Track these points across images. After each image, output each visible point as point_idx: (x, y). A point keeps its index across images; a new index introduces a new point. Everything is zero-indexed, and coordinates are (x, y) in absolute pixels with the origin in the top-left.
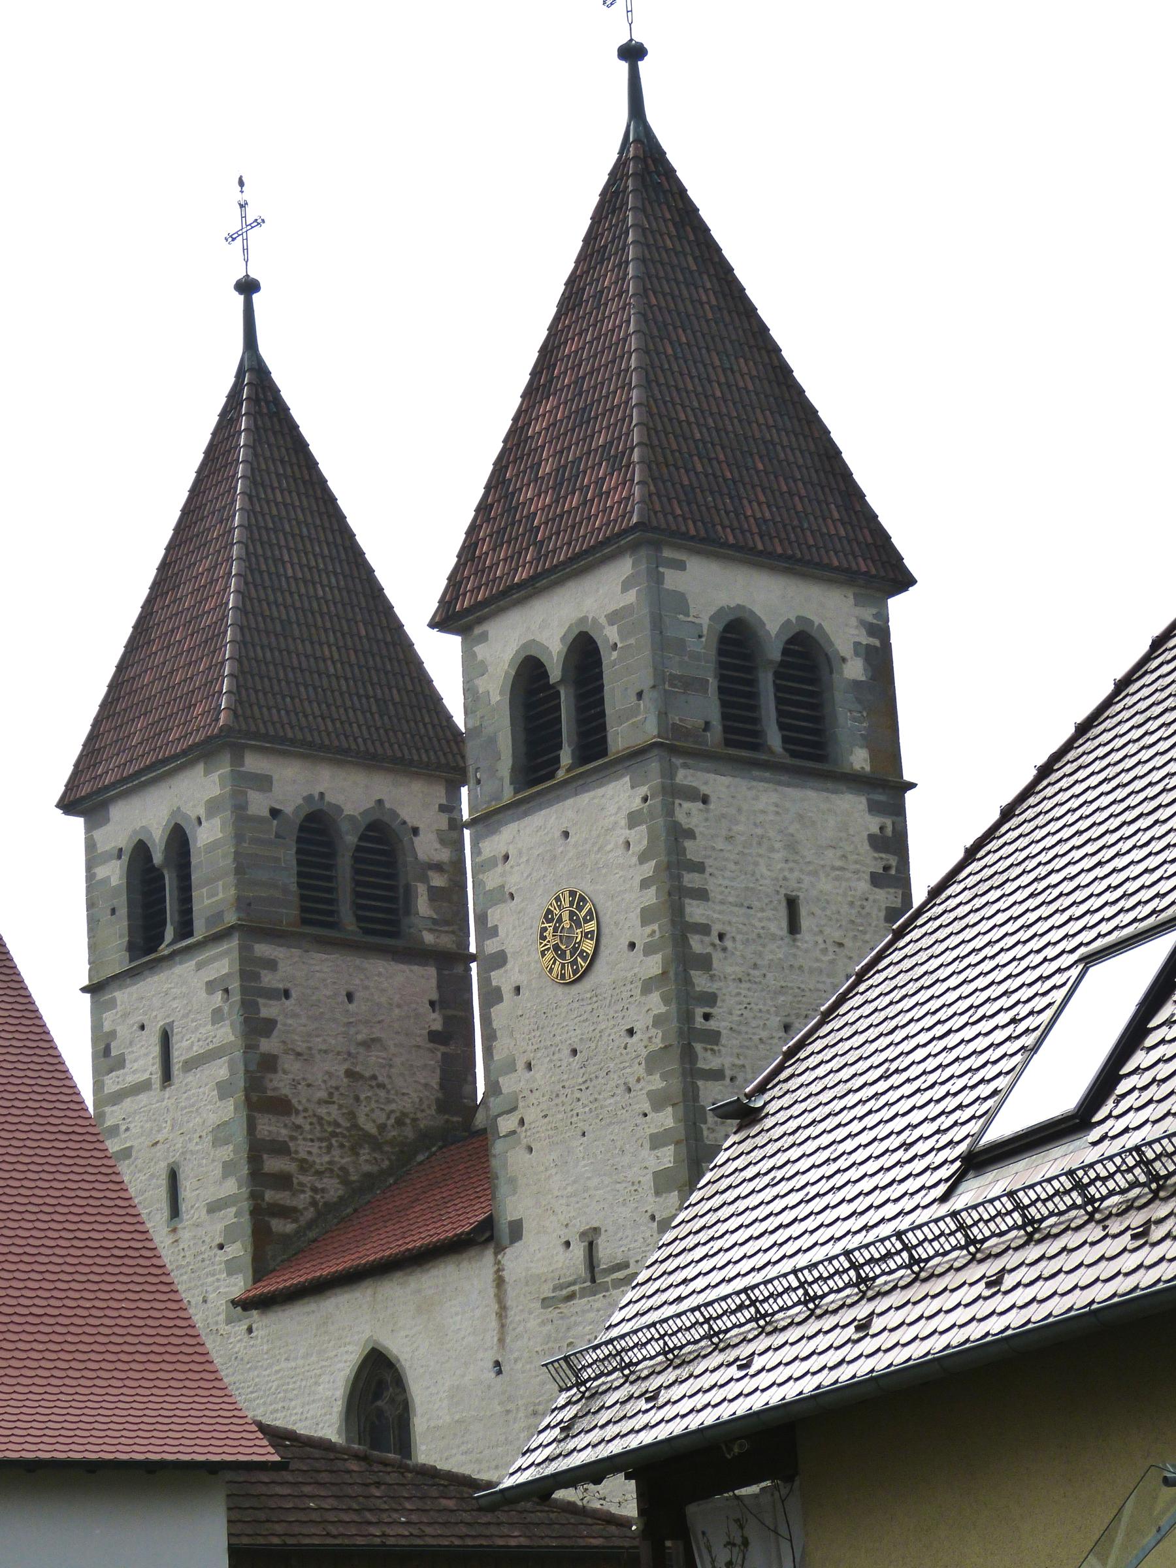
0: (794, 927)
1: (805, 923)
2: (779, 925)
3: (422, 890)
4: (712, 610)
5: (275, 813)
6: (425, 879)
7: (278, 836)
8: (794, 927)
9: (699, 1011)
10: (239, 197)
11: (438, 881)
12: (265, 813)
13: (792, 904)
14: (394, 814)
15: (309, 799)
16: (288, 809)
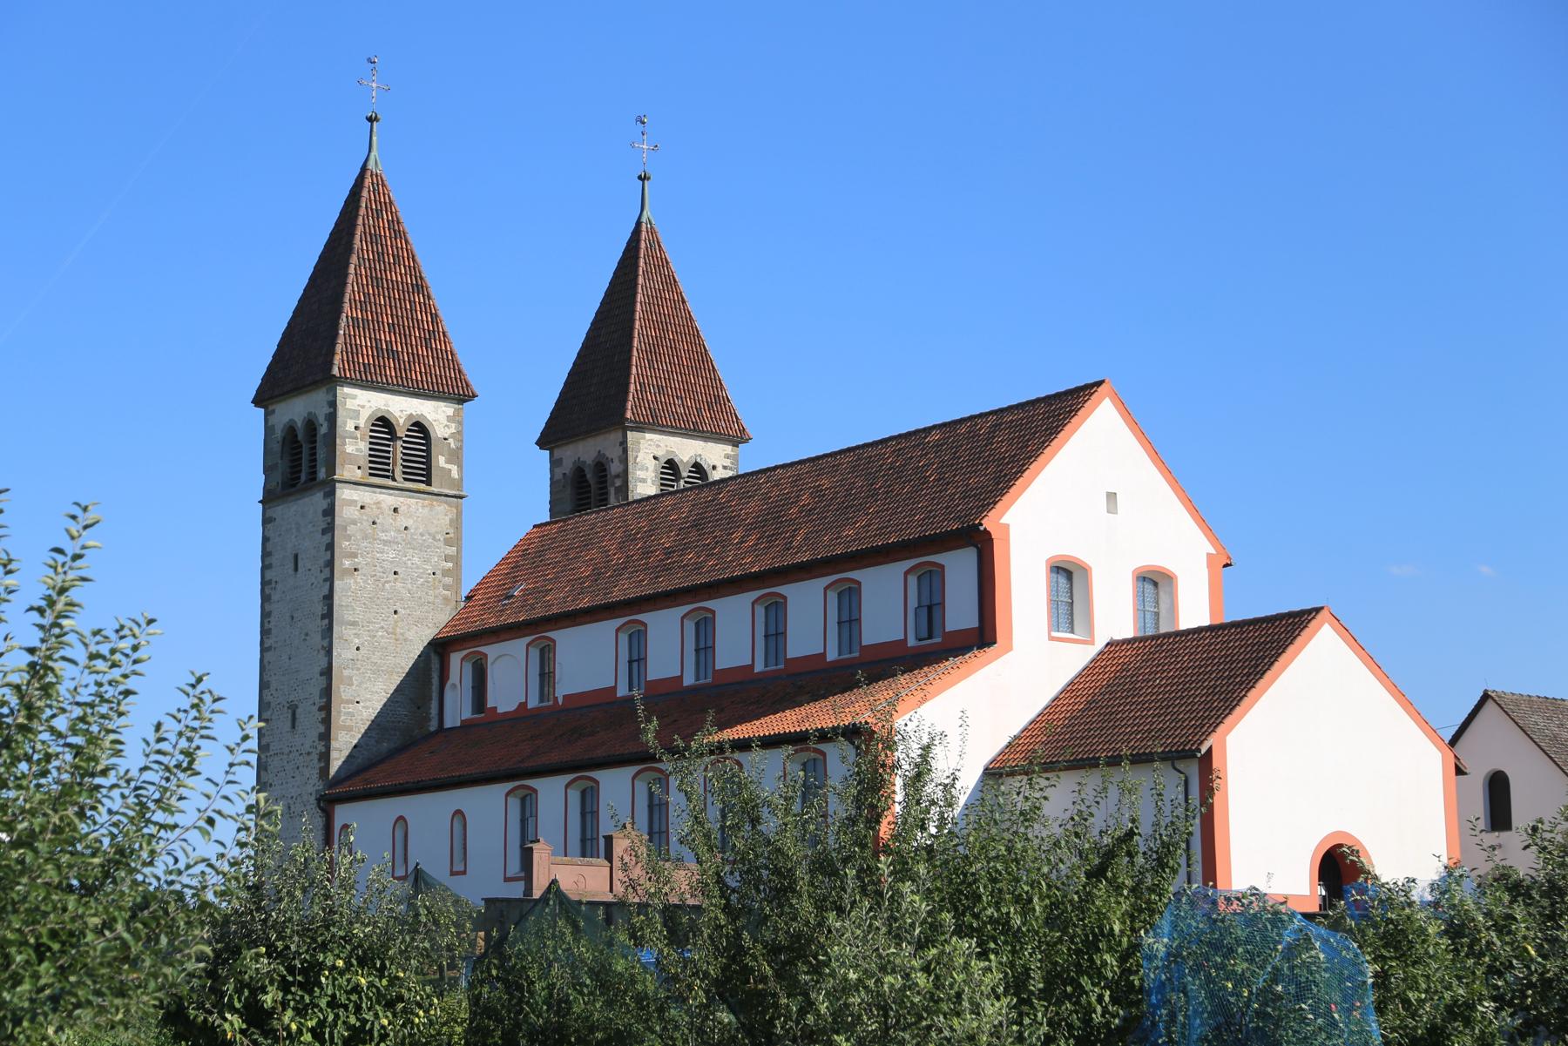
0: (296, 569)
1: (300, 564)
2: (291, 571)
3: (612, 491)
4: (282, 426)
5: (564, 474)
6: (613, 484)
7: (564, 487)
8: (296, 569)
9: (266, 621)
10: (642, 129)
11: (618, 483)
12: (561, 476)
13: (296, 557)
14: (604, 455)
15: (574, 463)
16: (567, 472)
